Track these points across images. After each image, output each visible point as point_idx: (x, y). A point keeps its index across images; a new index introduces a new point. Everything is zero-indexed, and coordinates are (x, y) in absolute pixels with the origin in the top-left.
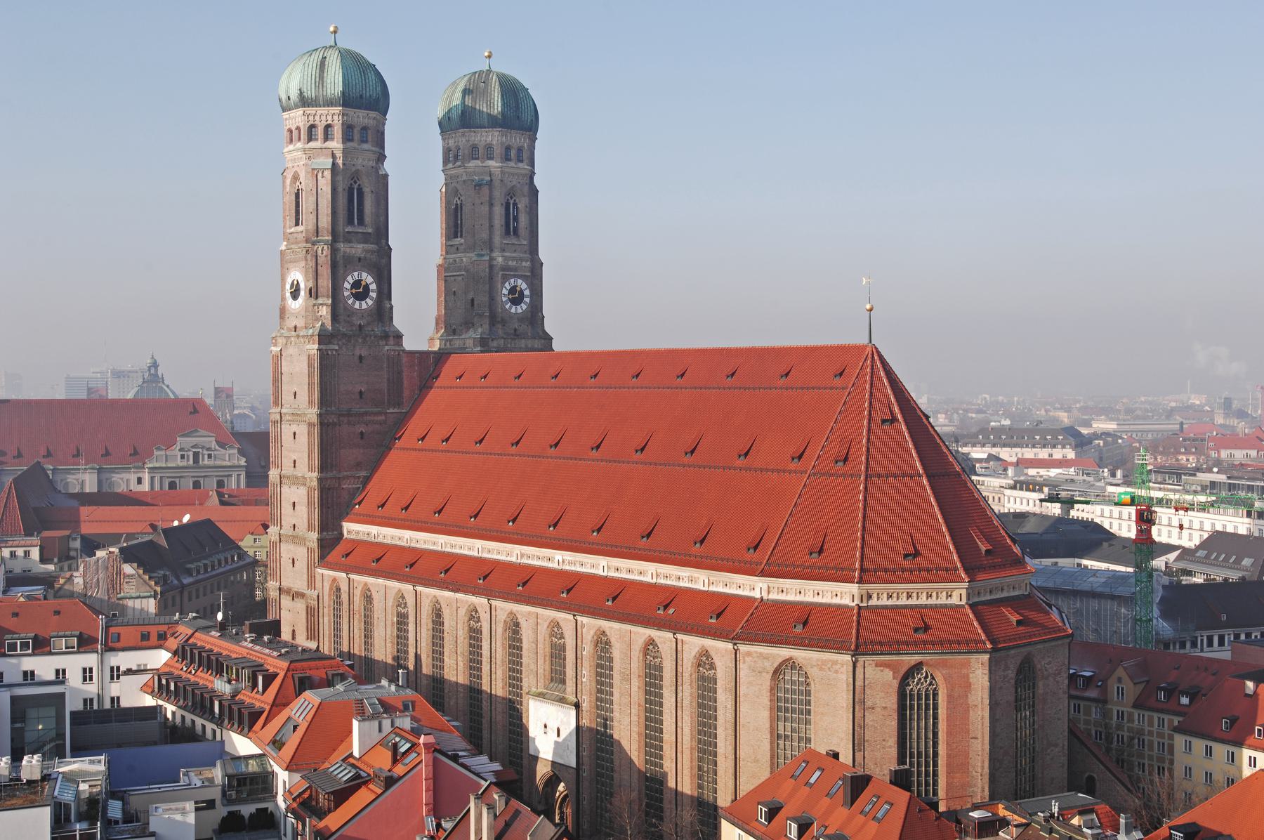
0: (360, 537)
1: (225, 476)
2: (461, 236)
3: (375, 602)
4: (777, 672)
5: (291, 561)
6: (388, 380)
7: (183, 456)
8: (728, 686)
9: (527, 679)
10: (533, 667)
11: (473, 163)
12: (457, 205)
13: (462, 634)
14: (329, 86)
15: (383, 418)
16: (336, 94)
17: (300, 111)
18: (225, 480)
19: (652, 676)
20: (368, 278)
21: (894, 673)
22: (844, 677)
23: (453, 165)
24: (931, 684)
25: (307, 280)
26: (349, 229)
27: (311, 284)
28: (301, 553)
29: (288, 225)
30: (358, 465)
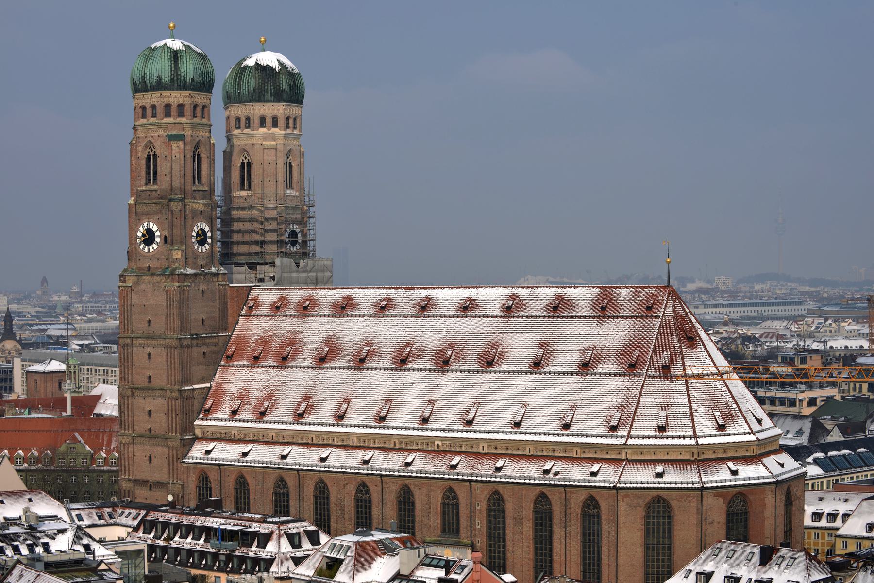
3: (252, 487)
5: (147, 458)
6: (219, 309)
8: (611, 518)
9: (420, 532)
11: (263, 130)
13: (350, 505)
14: (182, 74)
15: (215, 340)
16: (188, 81)
17: (157, 94)
21: (724, 500)
22: (695, 504)
23: (242, 131)
24: (743, 506)
26: (194, 188)
27: (166, 233)
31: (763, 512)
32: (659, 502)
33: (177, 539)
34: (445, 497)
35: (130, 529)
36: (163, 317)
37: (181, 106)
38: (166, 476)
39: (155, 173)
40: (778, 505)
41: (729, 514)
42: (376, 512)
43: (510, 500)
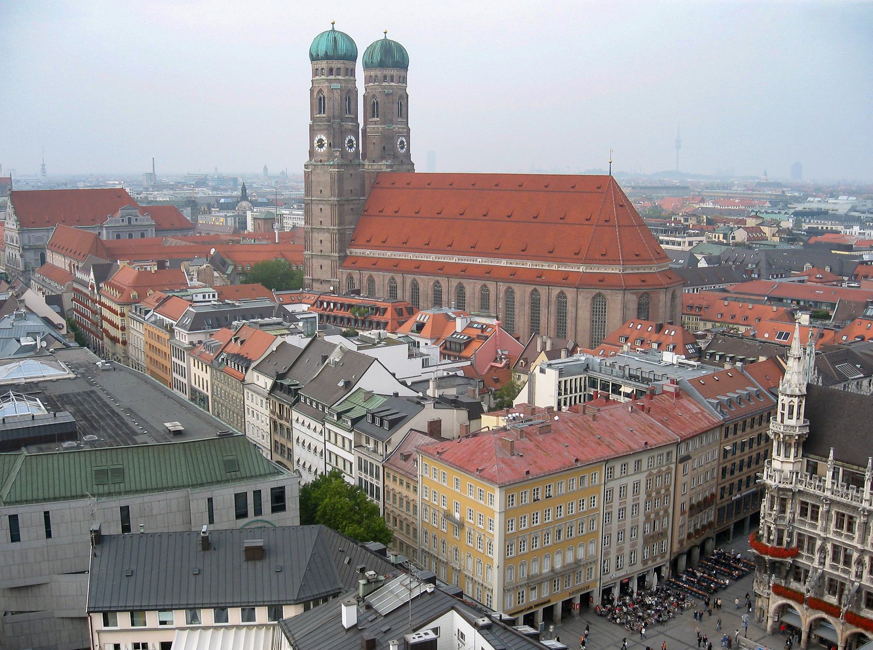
0: (359, 255)
1: (145, 230)
2: (377, 117)
4: (594, 298)
7: (123, 220)
10: (472, 303)
11: (384, 84)
12: (374, 102)
13: (430, 293)
15: (358, 202)
17: (325, 62)
18: (145, 232)
19: (535, 305)
20: (354, 139)
22: (620, 298)
25: (328, 139)
26: (346, 116)
28: (327, 263)
29: (315, 113)
30: (351, 223)
31: (658, 304)
32: (600, 296)
33: (335, 311)
34: (482, 290)
35: (309, 306)
36: (329, 188)
37: (339, 69)
38: (330, 276)
39: (324, 107)
40: (667, 300)
41: (639, 304)
42: (444, 297)
43: (518, 292)
